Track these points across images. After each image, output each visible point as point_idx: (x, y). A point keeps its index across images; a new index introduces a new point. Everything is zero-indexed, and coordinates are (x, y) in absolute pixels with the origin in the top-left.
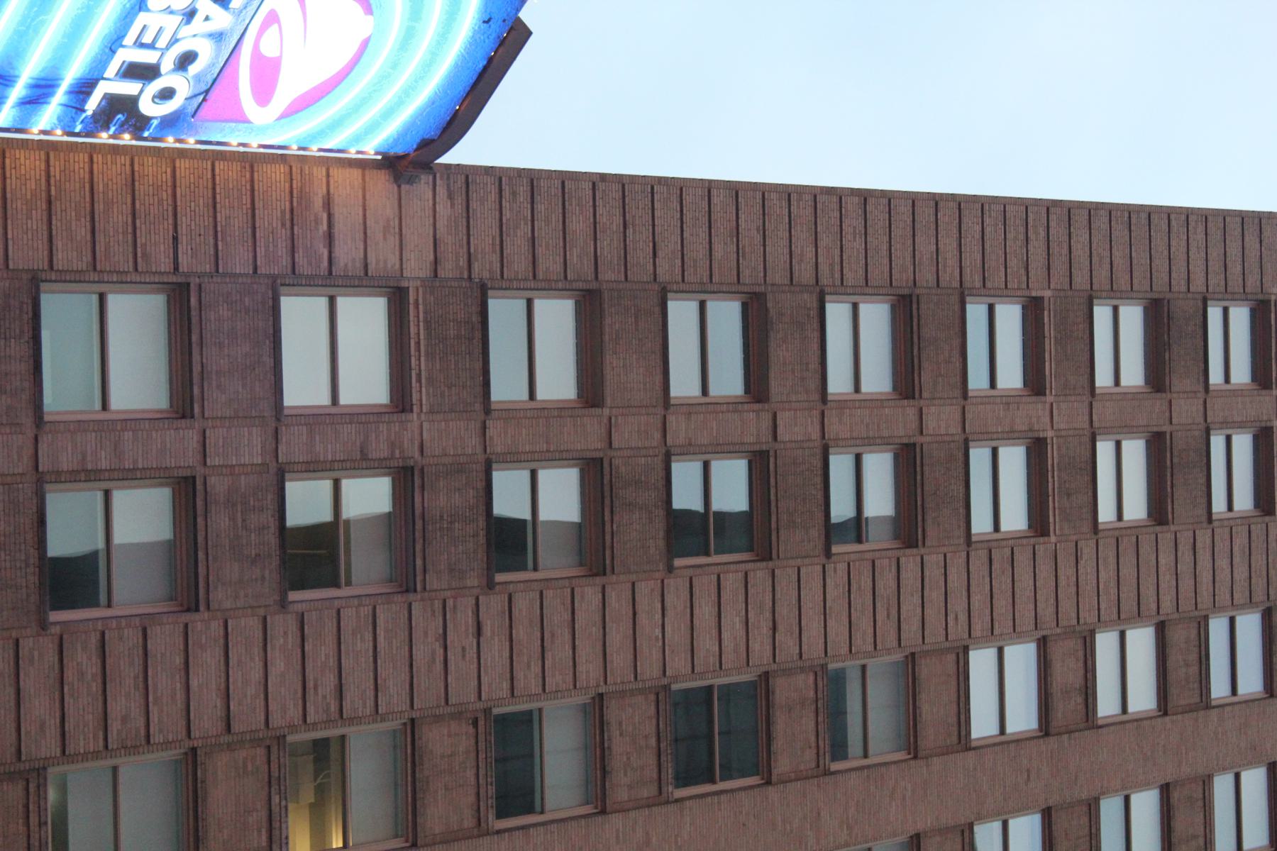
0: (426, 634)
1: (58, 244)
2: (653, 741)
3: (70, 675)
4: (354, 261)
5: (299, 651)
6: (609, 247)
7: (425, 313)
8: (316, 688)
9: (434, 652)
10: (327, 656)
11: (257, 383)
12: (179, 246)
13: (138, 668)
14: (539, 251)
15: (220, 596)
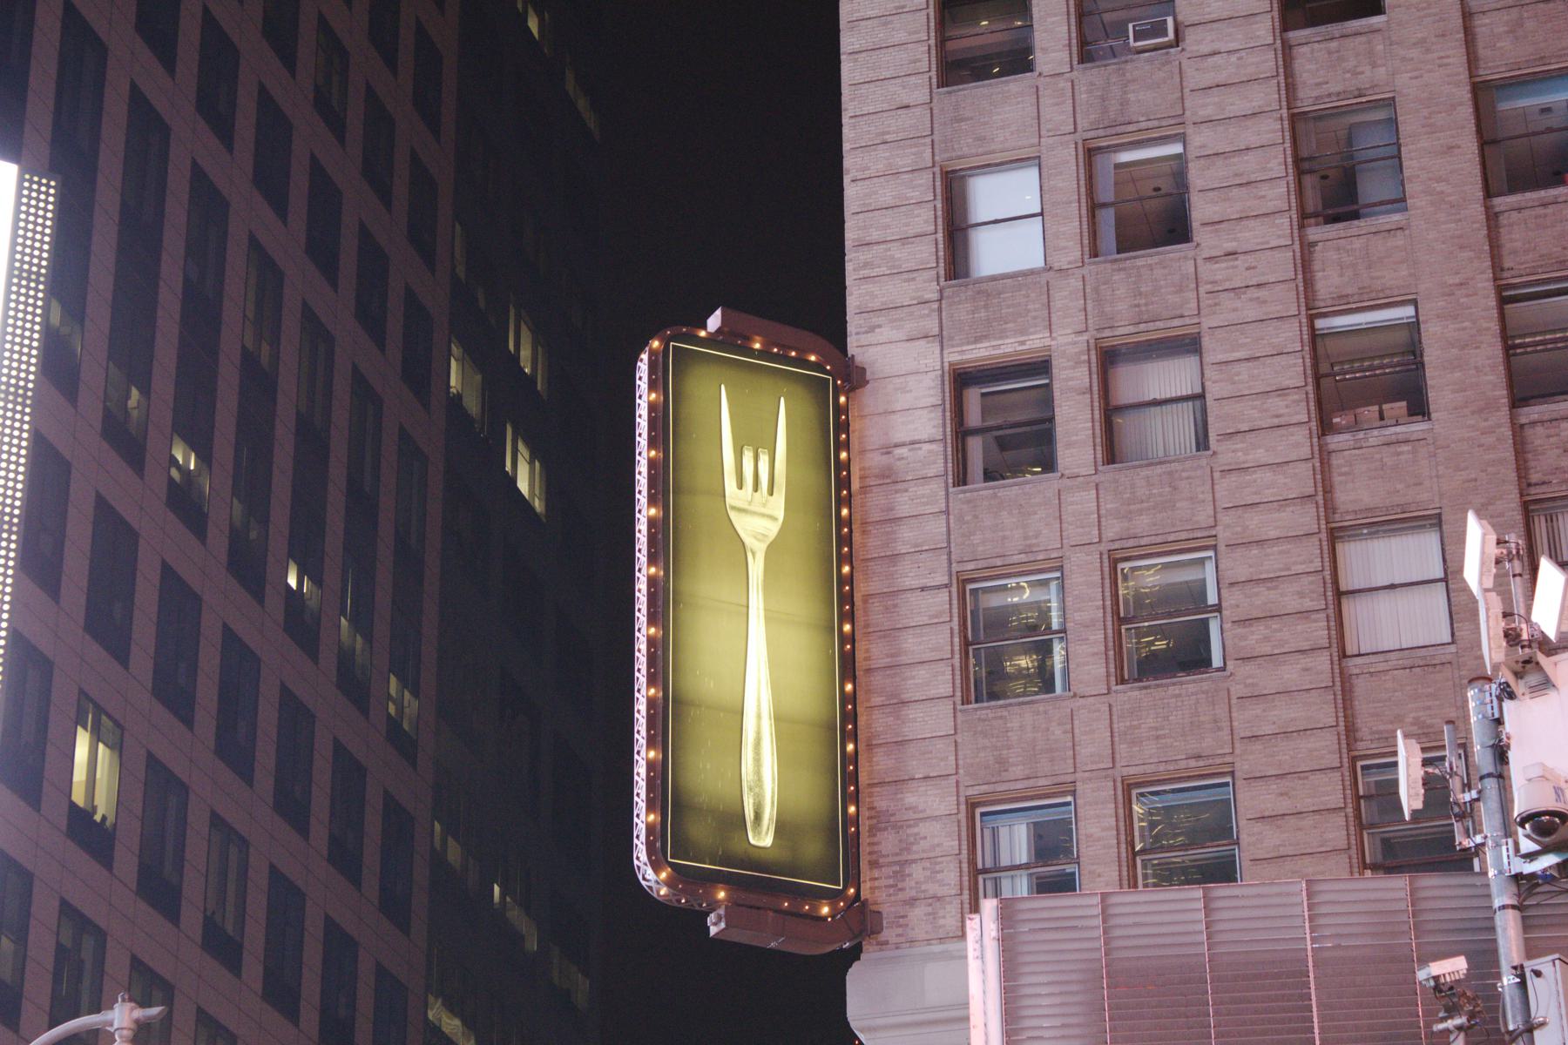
0: (1235, 310)
1: (933, 693)
2: (1334, 44)
3: (1267, 649)
4: (930, 420)
5: (1248, 435)
6: (905, 160)
7: (968, 343)
8: (1278, 416)
9: (1251, 300)
10: (1254, 408)
11: (1033, 501)
12: (928, 585)
13: (1261, 589)
14: (911, 232)
15: (1203, 517)
